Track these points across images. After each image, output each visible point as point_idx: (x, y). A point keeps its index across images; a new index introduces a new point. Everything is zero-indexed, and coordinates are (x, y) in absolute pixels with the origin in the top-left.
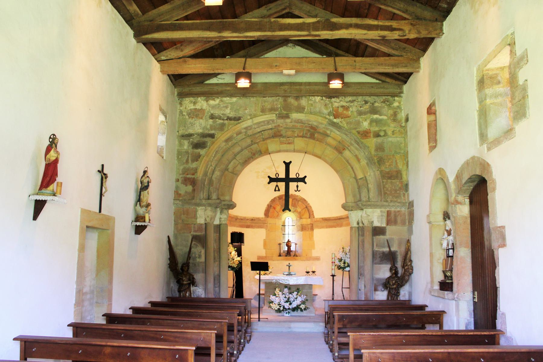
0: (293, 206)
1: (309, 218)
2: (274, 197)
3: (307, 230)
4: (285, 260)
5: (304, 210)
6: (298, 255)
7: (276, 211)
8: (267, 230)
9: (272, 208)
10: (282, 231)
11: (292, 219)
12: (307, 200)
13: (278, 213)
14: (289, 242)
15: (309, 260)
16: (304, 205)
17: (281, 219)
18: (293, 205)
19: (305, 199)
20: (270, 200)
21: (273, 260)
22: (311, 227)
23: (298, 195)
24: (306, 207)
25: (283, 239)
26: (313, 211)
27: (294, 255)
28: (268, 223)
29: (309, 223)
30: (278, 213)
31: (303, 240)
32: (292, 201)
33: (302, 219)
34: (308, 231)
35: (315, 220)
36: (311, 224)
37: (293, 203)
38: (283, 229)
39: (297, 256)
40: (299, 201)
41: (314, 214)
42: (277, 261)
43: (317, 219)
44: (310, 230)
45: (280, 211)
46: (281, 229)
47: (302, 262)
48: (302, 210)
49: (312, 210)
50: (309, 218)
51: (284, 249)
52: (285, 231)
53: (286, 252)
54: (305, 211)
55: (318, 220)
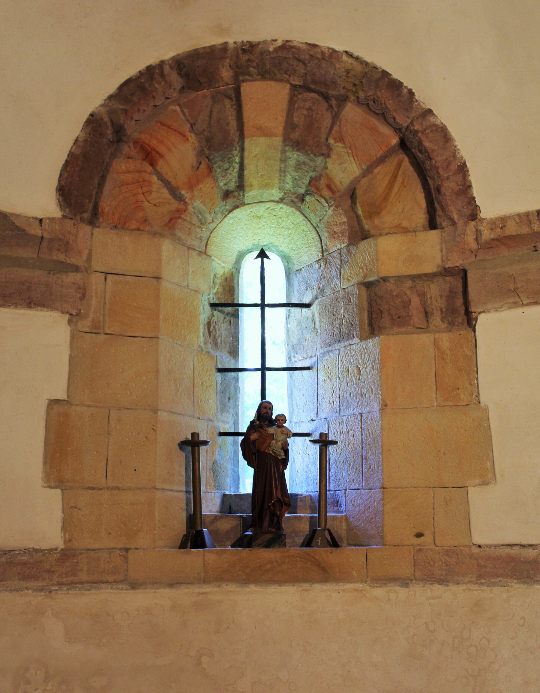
0: (298, 145)
1: (432, 225)
2: (142, 66)
3: (417, 318)
4: (232, 580)
5: (394, 160)
6: (340, 530)
7: (166, 183)
8: (85, 324)
9: (126, 149)
10: (215, 344)
11: (286, 259)
12: (407, 83)
13: (174, 192)
14: (271, 422)
15: (441, 581)
16: (385, 130)
17: (204, 253)
18: (295, 135)
19: (396, 75)
20: (112, 87)
21: (134, 586)
22: (450, 297)
23: (339, 48)
24: (403, 145)
25: (224, 408)
26: (463, 168)
27: (305, 528)
28: (87, 270)
29: (429, 268)
30: (180, 198)
31: (384, 406)
32: (292, 102)
33: (365, 236)
34: (419, 329)
35: (487, 235)
36: (446, 272)
37: (298, 118)
38: (223, 329)
39: (334, 543)
40: (343, 100)
41: (477, 192)
42: (166, 592)
43: (503, 220)
44: (436, 320)
45: (191, 187)
46: (202, 329)
47: (379, 592)
48: (368, 172)
49: (455, 153)
50: (432, 225)
51: (228, 481)
52: (234, 352)
53: (247, 504)
54: (395, 177)
55: (512, 229)
